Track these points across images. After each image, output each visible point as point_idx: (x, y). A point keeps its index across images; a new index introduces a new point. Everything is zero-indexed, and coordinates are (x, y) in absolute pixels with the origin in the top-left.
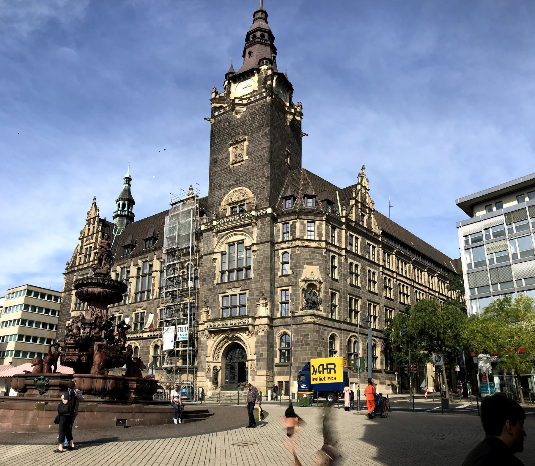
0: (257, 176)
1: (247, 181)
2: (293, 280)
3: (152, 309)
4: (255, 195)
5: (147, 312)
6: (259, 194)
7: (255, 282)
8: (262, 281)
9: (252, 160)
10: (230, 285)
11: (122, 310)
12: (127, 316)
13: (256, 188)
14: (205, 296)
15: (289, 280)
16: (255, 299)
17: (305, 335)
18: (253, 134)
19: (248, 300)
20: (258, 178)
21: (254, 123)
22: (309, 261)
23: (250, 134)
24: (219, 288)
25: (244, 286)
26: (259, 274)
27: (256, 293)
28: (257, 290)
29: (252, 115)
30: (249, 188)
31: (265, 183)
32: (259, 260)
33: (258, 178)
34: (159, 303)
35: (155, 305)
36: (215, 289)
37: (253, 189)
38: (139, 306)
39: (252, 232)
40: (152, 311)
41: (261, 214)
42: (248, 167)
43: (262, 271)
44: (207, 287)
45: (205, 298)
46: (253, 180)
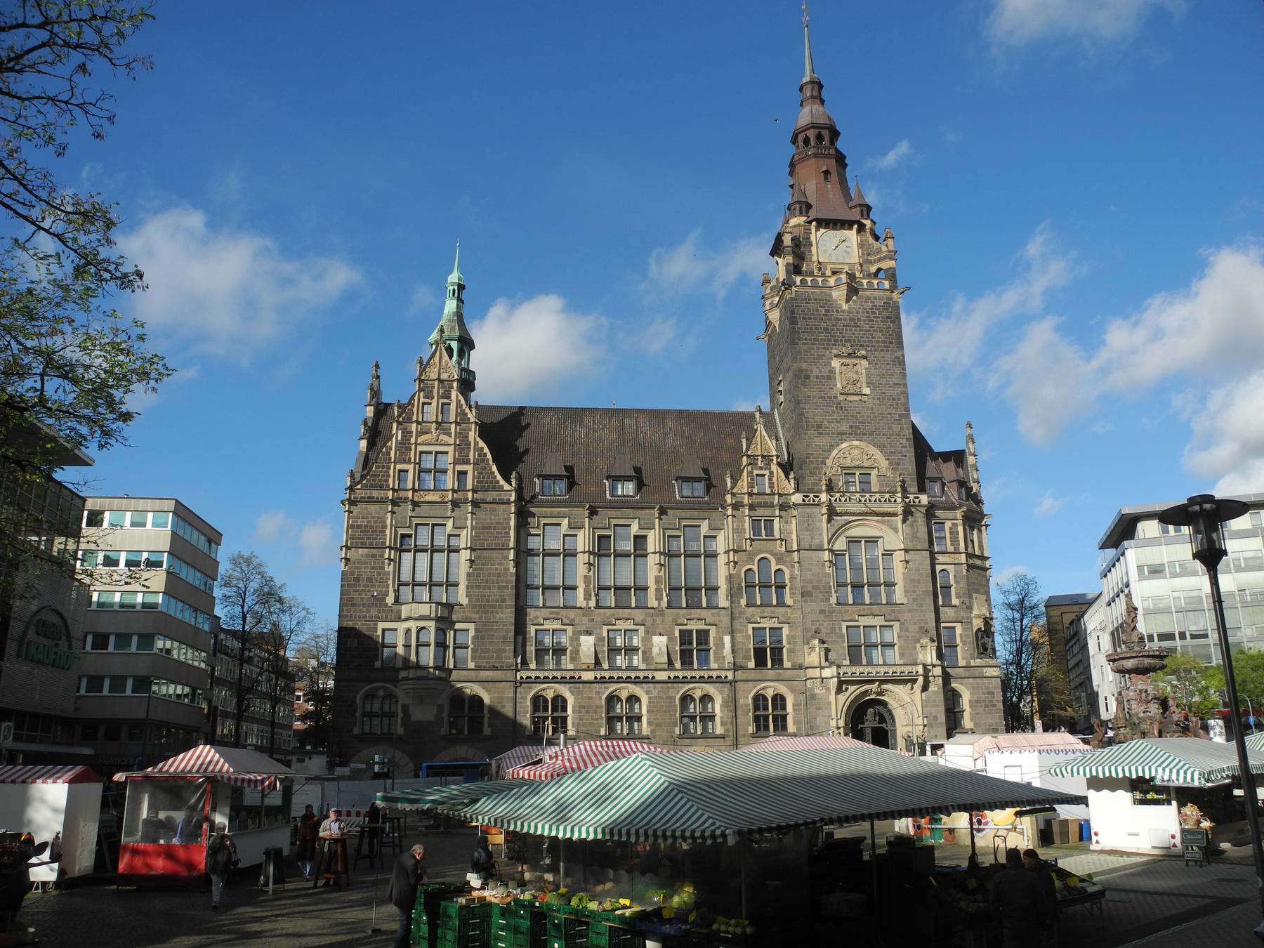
0: (891, 432)
1: (873, 434)
2: (963, 614)
3: (660, 627)
4: (891, 464)
5: (647, 632)
6: (898, 464)
7: (910, 611)
8: (921, 611)
9: (879, 399)
10: (864, 610)
11: (567, 617)
12: (588, 633)
13: (892, 452)
14: (812, 621)
15: (956, 612)
16: (912, 636)
17: (989, 693)
18: (875, 350)
19: (899, 637)
20: (893, 435)
21: (874, 331)
22: (976, 587)
23: (869, 349)
24: (840, 612)
25: (891, 615)
26: (914, 600)
27: (914, 629)
28: (914, 624)
29: (868, 312)
30: (881, 447)
31: (906, 447)
32: (912, 577)
33: (893, 435)
34: (679, 618)
35: (669, 620)
36: (832, 612)
37: (886, 453)
38: (620, 616)
39: (897, 529)
40: (663, 631)
41: (910, 502)
42: (872, 408)
43: (919, 595)
44: (813, 606)
45: (813, 625)
46: (883, 435)
